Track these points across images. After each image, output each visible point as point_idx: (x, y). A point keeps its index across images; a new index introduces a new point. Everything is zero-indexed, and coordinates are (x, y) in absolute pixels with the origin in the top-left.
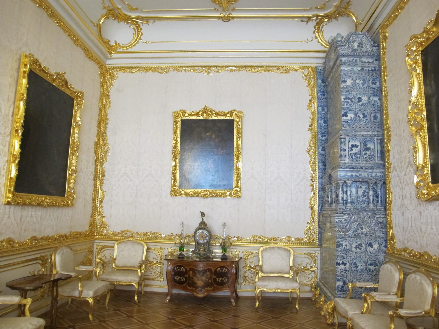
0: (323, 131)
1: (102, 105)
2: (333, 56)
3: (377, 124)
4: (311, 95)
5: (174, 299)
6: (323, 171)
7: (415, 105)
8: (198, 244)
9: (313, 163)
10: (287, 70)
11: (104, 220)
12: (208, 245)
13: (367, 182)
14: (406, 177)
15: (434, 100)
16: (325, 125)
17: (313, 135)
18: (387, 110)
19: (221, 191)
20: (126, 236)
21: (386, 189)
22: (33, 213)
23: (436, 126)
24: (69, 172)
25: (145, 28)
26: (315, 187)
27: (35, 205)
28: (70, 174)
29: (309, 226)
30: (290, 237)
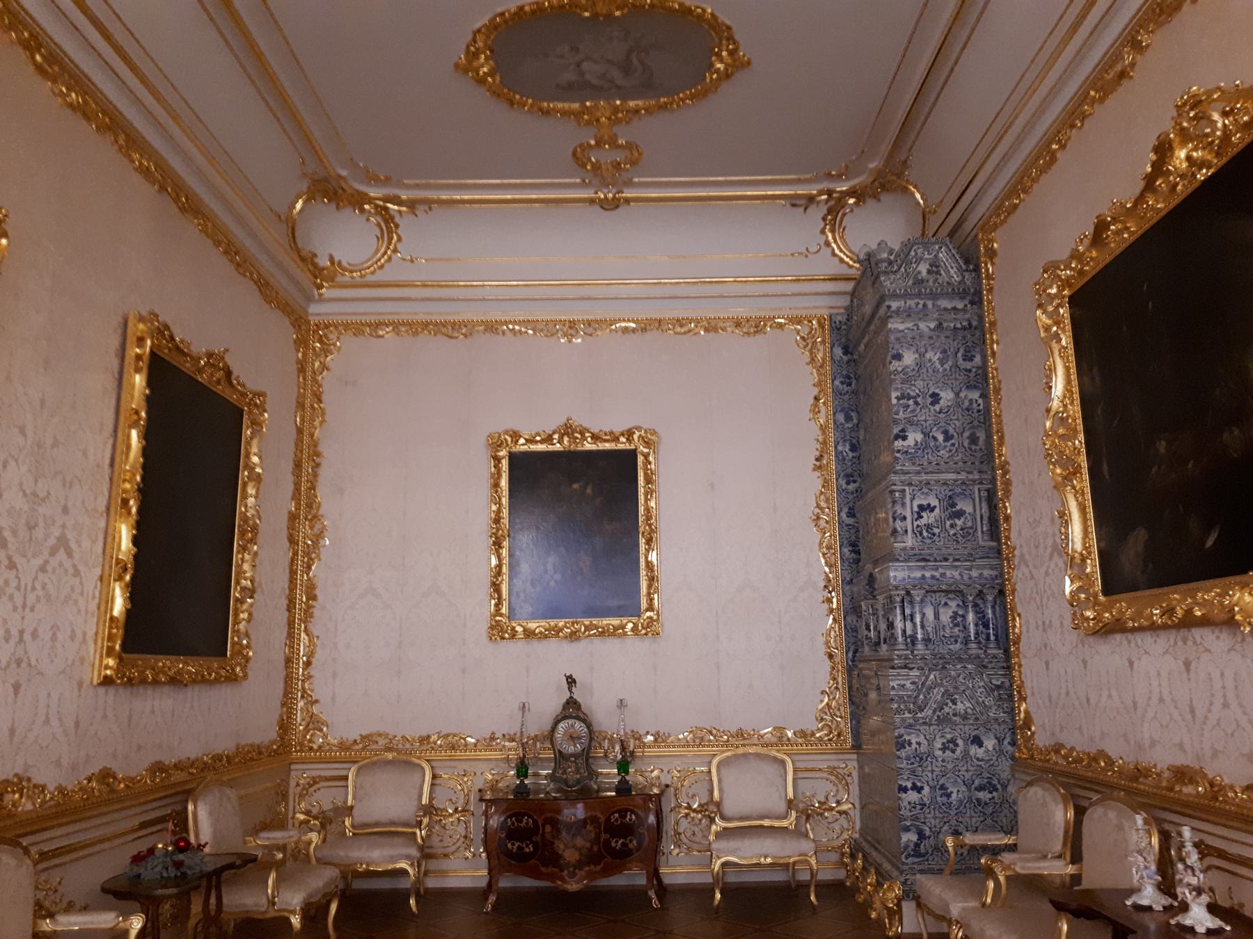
0: (849, 471)
1: (302, 420)
3: (978, 455)
4: (818, 384)
5: (510, 903)
8: (561, 757)
9: (829, 548)
10: (757, 326)
11: (315, 709)
12: (586, 757)
13: (960, 593)
14: (1048, 580)
17: (826, 481)
18: (1000, 423)
20: (375, 747)
21: (1005, 607)
22: (156, 703)
23: (1105, 467)
24: (235, 593)
25: (407, 224)
27: (164, 683)
29: (826, 700)
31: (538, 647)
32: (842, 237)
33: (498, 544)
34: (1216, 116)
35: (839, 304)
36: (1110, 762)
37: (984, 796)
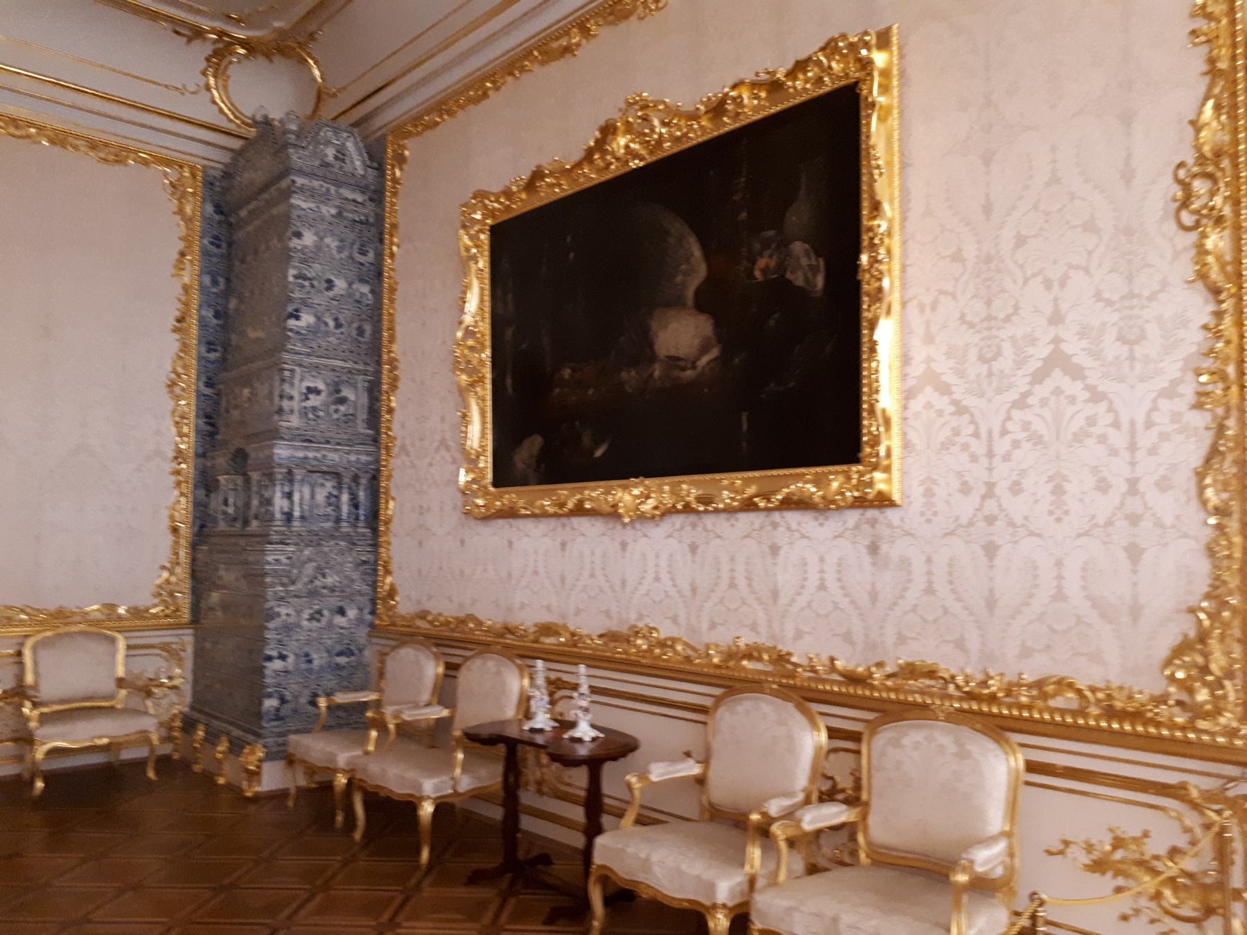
3: (364, 347)
7: (469, 333)
10: (118, 155)
13: (337, 475)
15: (509, 333)
16: (220, 322)
18: (391, 321)
23: (509, 381)
32: (225, 87)
34: (656, 122)
35: (222, 160)
36: (480, 623)
37: (342, 660)
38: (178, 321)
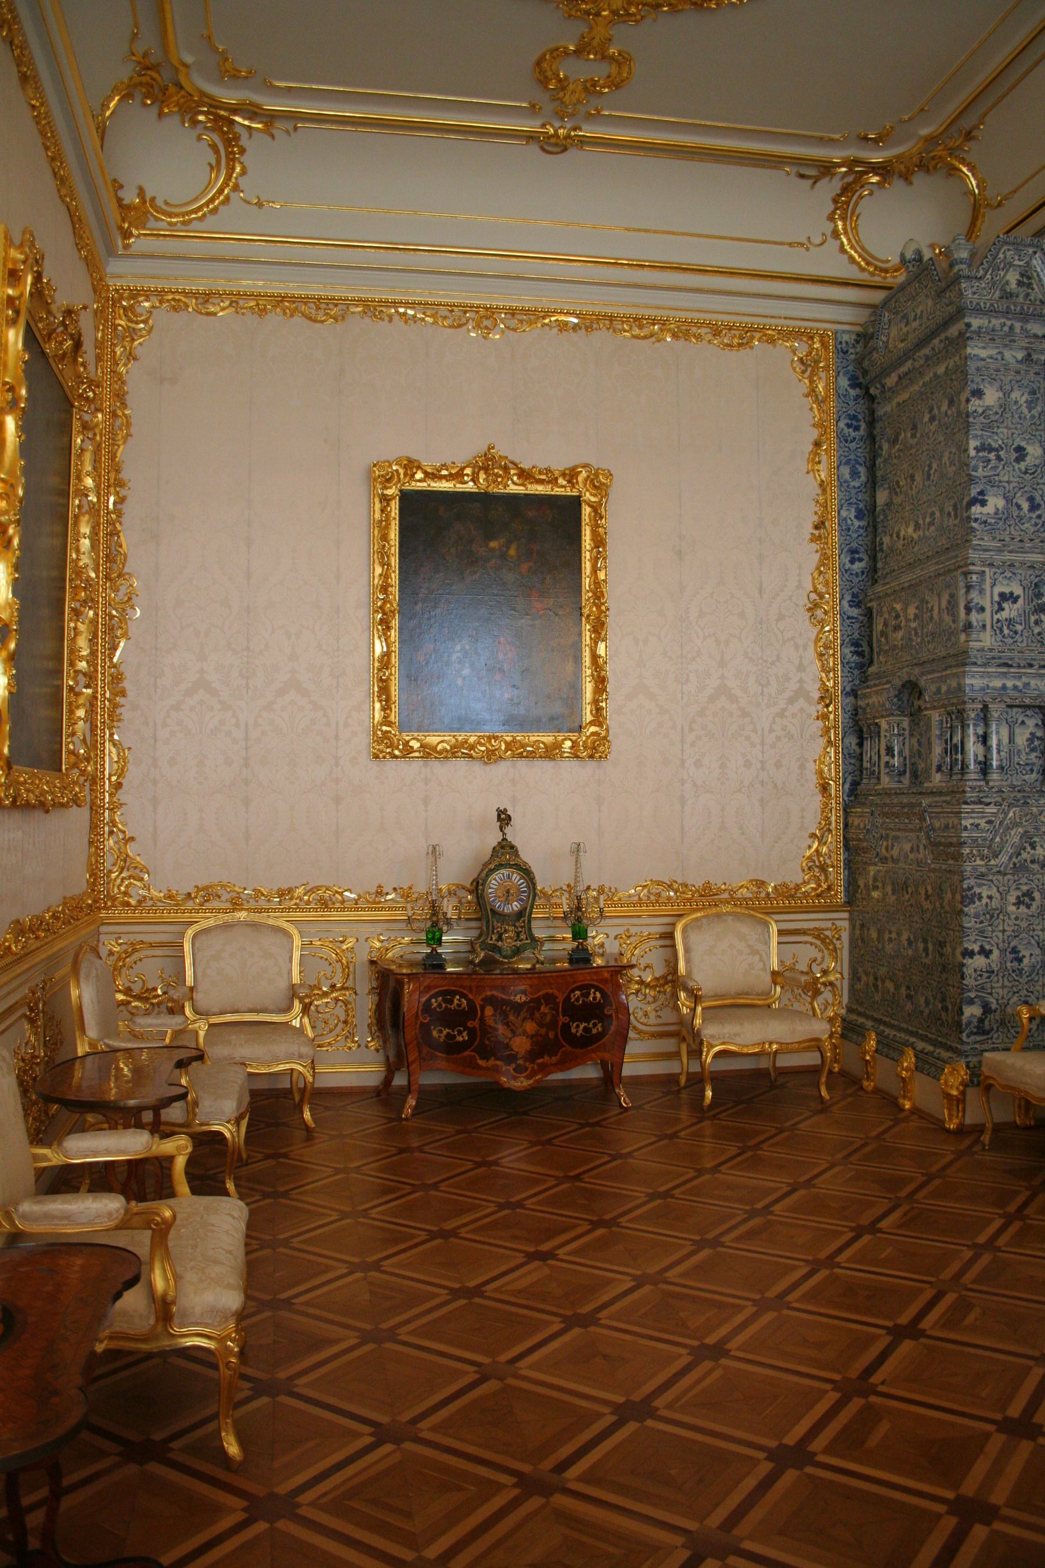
0: (854, 545)
2: (925, 306)
6: (856, 672)
10: (743, 335)
16: (861, 523)
17: (825, 557)
19: (544, 739)
26: (832, 723)
28: (71, 689)
30: (761, 884)
31: (440, 769)
33: (386, 624)
38: (816, 527)
